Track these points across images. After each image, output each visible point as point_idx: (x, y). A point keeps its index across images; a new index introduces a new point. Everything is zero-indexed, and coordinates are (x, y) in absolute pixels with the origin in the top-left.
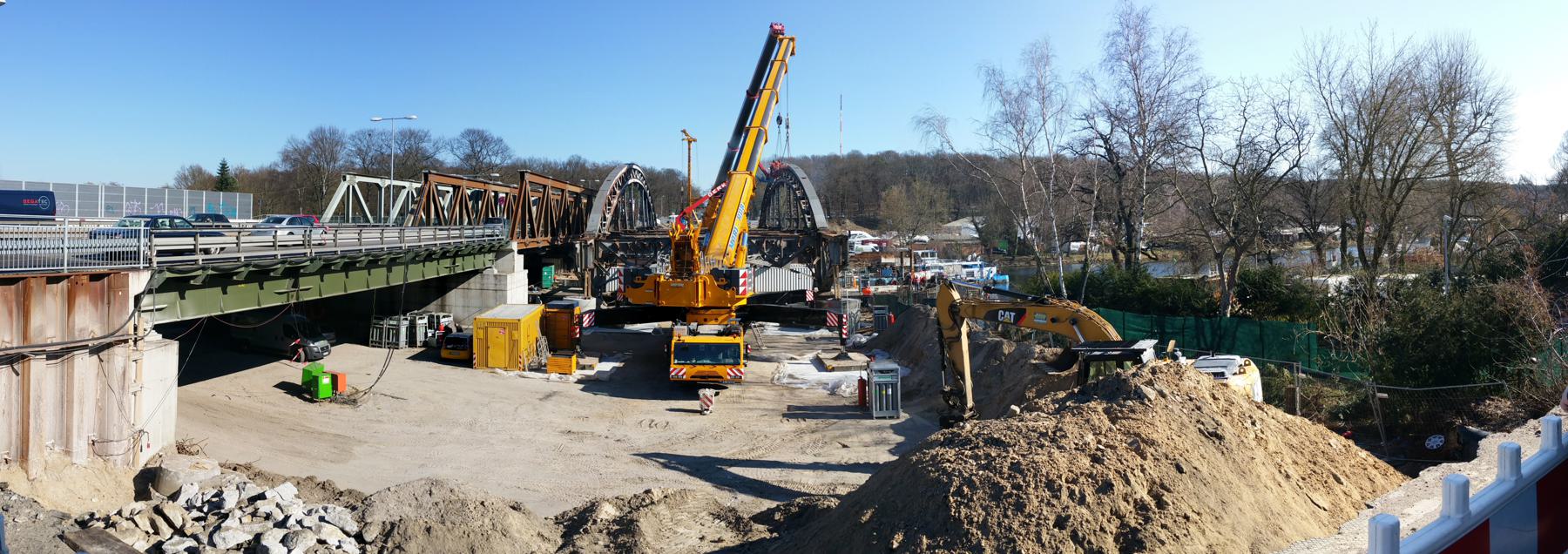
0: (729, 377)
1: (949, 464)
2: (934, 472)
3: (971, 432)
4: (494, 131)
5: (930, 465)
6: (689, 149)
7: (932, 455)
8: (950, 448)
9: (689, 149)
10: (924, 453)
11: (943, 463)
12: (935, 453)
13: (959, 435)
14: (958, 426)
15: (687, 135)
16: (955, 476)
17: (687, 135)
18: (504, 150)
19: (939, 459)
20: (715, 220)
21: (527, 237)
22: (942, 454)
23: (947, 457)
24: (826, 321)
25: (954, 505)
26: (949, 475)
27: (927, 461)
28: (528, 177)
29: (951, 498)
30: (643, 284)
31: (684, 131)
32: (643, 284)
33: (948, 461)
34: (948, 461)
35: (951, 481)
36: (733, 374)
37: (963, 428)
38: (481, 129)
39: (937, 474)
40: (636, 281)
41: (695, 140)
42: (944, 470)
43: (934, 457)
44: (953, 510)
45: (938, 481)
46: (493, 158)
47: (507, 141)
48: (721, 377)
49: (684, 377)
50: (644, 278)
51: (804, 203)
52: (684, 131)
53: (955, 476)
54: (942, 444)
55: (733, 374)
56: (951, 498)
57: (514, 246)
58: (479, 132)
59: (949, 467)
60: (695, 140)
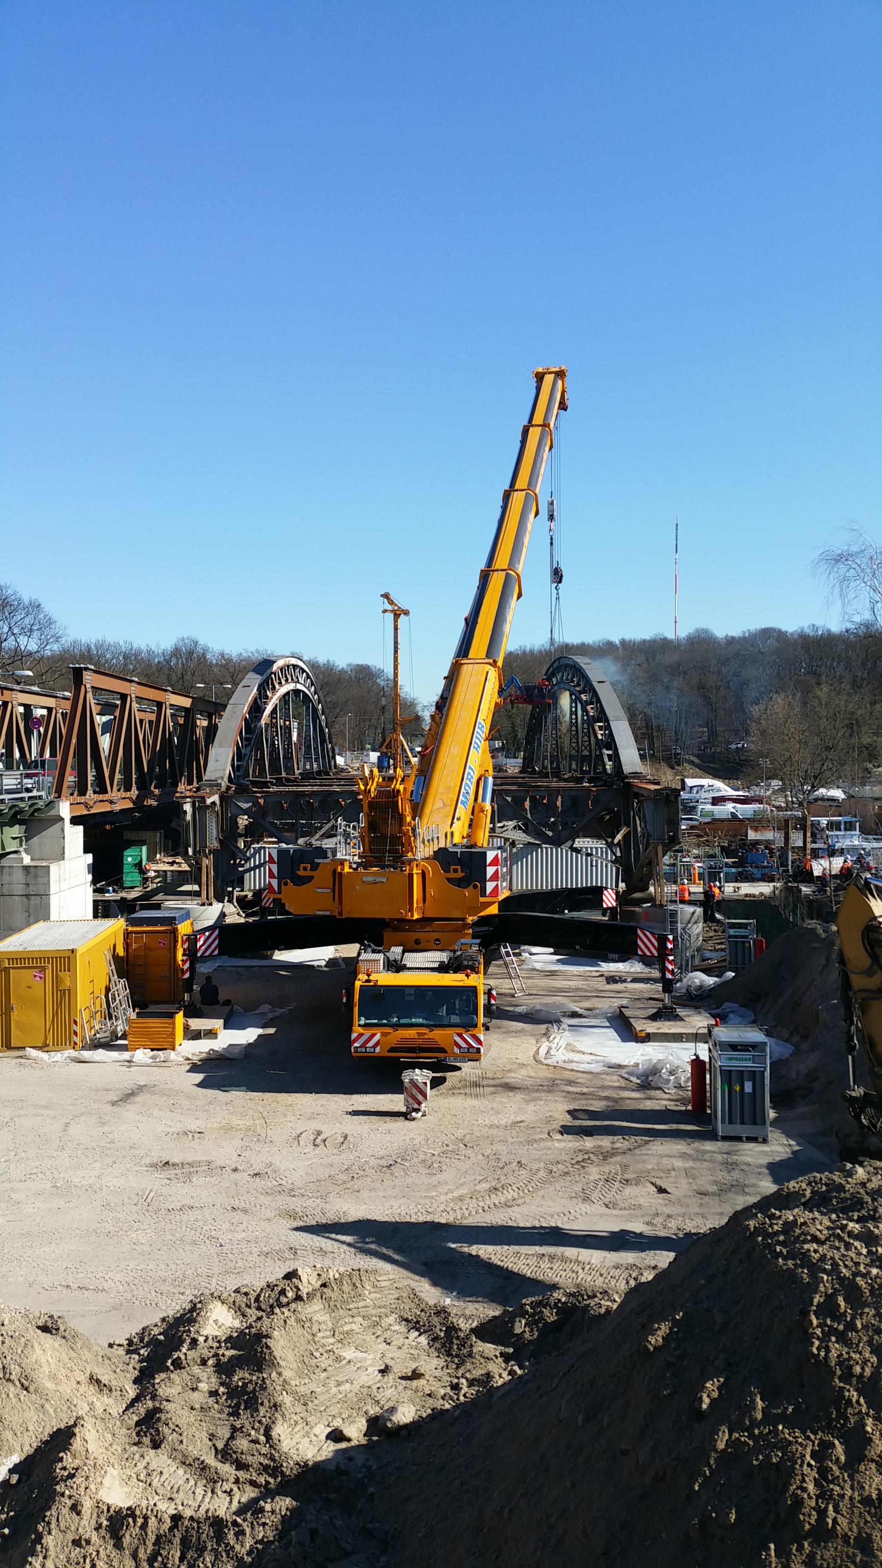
0: (457, 1050)
1: (815, 1245)
2: (785, 1258)
3: (863, 1185)
5: (783, 1244)
6: (396, 629)
7: (786, 1223)
8: (822, 1214)
9: (396, 629)
10: (772, 1217)
11: (805, 1241)
12: (791, 1218)
13: (841, 1188)
14: (842, 1170)
15: (391, 602)
16: (825, 1271)
17: (391, 602)
19: (798, 1231)
22: (805, 1223)
23: (812, 1230)
24: (637, 946)
25: (818, 1331)
26: (815, 1269)
27: (777, 1233)
28: (89, 679)
29: (813, 1318)
31: (386, 596)
33: (815, 1239)
34: (815, 1239)
35: (817, 1281)
36: (463, 1045)
37: (850, 1174)
39: (790, 1263)
41: (406, 613)
42: (806, 1254)
43: (789, 1227)
44: (817, 1343)
45: (791, 1276)
47: (50, 607)
48: (443, 1050)
49: (378, 1050)
51: (600, 728)
52: (386, 596)
53: (825, 1271)
54: (808, 1206)
55: (463, 1045)
56: (813, 1318)
57: (65, 809)
59: (815, 1251)
60: (406, 613)
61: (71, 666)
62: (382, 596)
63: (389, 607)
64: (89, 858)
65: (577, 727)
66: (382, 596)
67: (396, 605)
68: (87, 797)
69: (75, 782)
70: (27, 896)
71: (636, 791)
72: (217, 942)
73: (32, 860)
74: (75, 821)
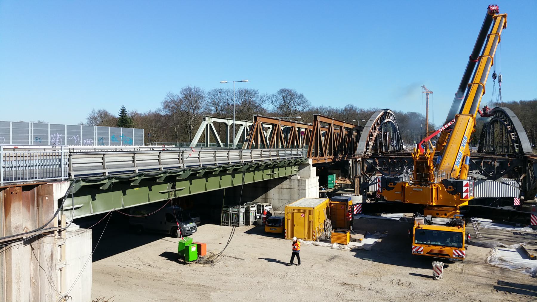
4: (298, 91)
6: (427, 99)
9: (427, 99)
15: (426, 89)
17: (426, 89)
18: (303, 102)
20: (446, 147)
21: (318, 156)
28: (318, 118)
30: (394, 188)
31: (423, 87)
32: (394, 188)
38: (290, 89)
40: (389, 186)
41: (431, 93)
46: (297, 107)
47: (306, 96)
50: (395, 184)
51: (513, 135)
52: (423, 87)
57: (310, 161)
58: (288, 90)
60: (431, 93)
61: (313, 114)
62: (422, 87)
63: (425, 91)
64: (318, 177)
65: (502, 135)
66: (422, 87)
67: (428, 90)
68: (317, 157)
69: (314, 153)
70: (299, 189)
71: (530, 160)
72: (361, 209)
73: (300, 178)
74: (314, 165)
